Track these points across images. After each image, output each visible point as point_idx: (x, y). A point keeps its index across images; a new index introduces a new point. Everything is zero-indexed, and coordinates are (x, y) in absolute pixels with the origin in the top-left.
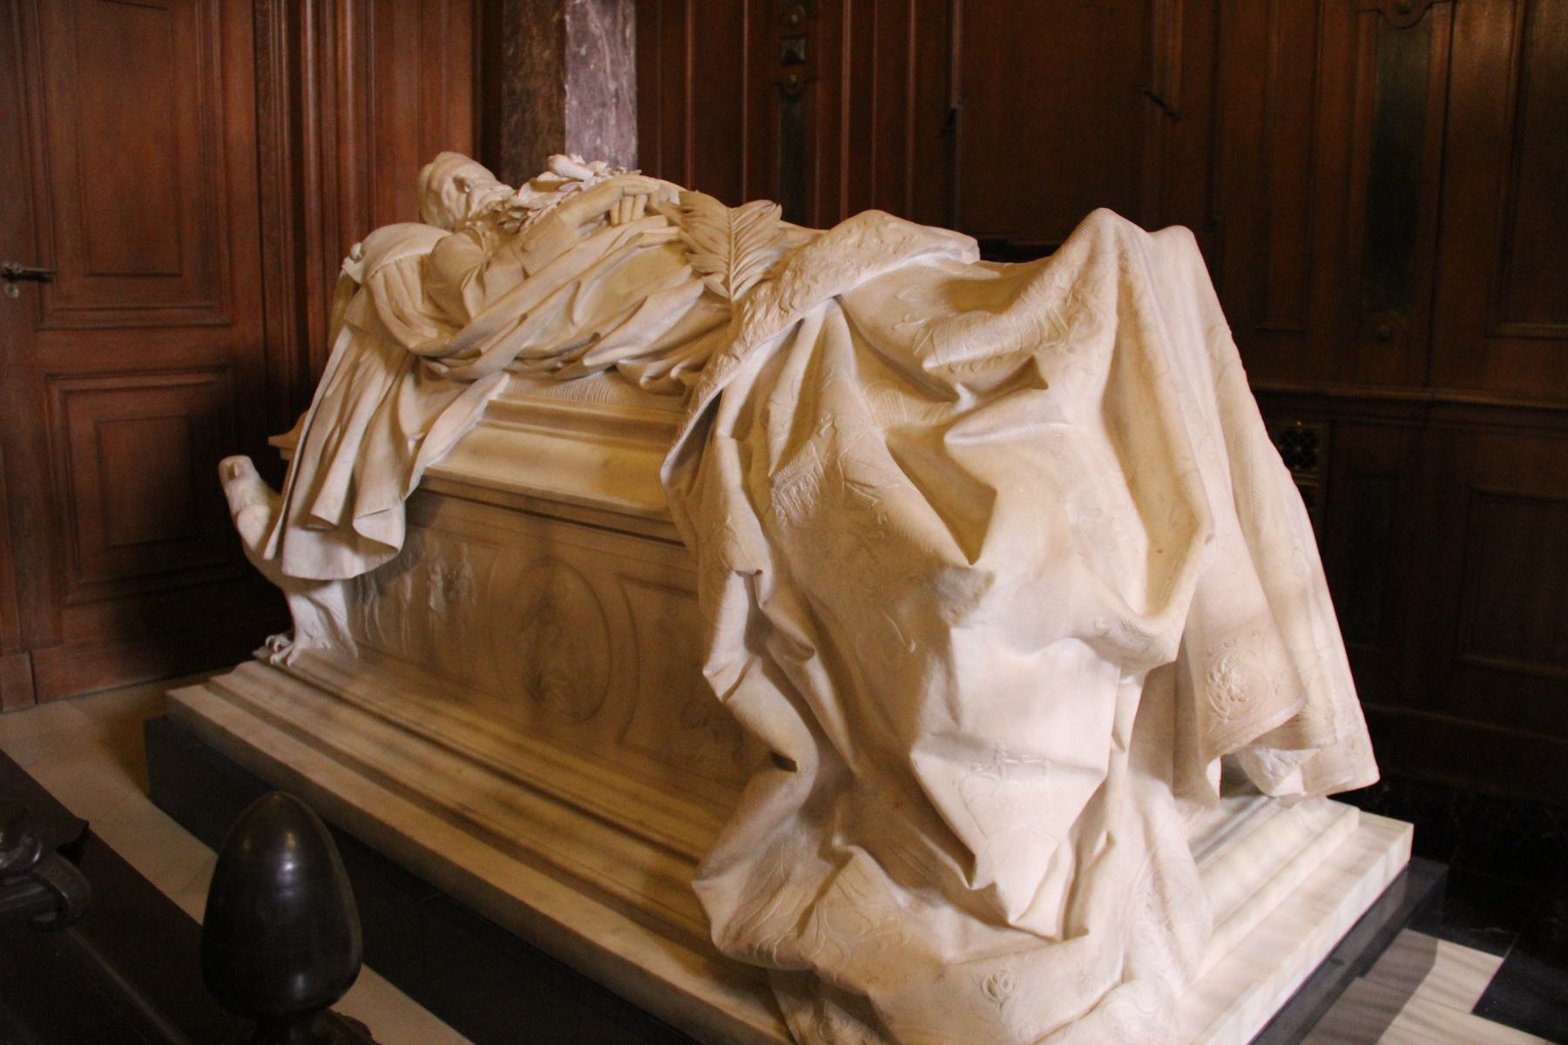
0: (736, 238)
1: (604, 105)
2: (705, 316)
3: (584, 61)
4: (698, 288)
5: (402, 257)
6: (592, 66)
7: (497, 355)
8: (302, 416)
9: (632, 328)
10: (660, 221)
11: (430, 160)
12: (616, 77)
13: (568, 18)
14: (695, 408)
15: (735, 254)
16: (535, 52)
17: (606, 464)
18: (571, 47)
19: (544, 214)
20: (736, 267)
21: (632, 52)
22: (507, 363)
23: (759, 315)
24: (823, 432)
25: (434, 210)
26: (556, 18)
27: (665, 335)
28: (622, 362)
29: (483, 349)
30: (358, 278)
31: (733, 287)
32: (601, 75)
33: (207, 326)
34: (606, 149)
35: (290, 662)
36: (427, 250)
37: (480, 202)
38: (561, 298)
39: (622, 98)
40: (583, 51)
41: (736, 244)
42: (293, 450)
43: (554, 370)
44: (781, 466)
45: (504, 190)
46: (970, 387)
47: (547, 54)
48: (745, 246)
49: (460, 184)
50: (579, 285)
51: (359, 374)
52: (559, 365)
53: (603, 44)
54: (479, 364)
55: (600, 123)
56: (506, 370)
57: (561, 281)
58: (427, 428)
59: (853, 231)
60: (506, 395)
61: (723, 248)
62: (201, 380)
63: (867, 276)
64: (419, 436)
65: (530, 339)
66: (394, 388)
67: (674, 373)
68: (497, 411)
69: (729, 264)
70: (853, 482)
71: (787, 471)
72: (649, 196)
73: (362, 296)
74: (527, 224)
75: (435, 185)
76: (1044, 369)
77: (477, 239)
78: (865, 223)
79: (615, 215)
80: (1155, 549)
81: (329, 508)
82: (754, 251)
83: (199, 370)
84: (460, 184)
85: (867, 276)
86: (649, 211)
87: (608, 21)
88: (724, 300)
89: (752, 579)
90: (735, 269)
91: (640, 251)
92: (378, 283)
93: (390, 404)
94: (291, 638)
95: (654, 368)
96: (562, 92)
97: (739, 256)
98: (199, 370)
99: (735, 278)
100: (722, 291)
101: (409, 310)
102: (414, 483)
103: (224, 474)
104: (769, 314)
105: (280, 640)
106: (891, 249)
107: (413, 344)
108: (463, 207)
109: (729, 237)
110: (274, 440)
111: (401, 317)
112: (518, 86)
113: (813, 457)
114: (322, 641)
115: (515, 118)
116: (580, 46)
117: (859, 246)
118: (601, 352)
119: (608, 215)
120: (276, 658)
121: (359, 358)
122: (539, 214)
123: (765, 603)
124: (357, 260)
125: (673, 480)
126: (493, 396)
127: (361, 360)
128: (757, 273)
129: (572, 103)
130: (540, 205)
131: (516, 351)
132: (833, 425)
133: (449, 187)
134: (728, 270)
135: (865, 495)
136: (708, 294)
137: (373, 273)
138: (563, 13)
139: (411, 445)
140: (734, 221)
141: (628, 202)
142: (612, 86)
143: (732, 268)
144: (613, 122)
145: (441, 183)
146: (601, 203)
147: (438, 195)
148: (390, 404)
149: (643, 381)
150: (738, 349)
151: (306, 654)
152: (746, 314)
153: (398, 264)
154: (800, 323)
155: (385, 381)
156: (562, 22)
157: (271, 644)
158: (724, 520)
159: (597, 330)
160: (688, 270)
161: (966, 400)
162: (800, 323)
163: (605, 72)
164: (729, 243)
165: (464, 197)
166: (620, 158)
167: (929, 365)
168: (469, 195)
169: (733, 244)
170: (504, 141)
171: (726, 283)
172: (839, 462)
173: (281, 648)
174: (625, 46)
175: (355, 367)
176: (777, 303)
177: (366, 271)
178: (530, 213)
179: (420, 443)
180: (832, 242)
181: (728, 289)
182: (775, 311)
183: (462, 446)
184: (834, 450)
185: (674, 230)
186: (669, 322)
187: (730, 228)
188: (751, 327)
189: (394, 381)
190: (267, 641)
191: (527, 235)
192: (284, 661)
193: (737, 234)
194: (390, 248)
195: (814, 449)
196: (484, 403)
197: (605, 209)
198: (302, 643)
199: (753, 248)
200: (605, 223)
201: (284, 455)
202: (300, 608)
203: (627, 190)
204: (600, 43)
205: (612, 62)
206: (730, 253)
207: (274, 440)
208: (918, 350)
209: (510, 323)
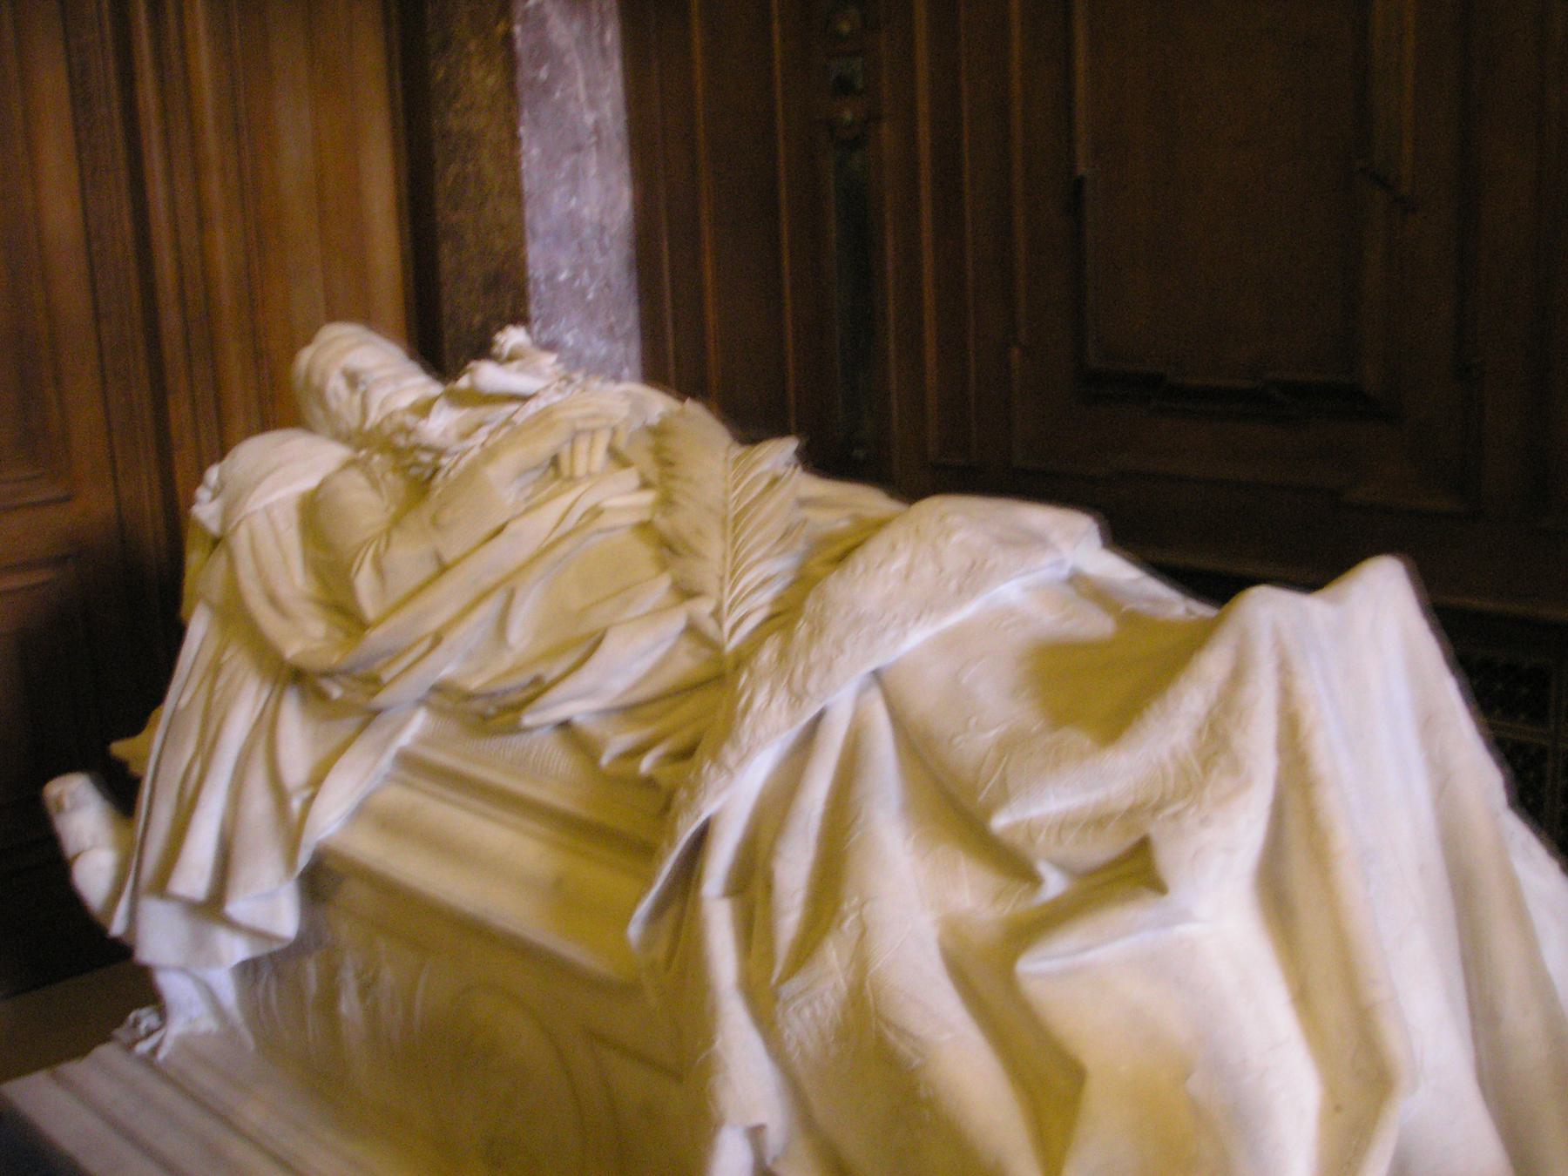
0: (735, 527)
1: (578, 148)
2: (687, 664)
3: (547, 88)
4: (677, 622)
5: (274, 498)
6: (558, 95)
7: (403, 690)
8: (153, 715)
9: (587, 677)
10: (630, 478)
11: (308, 341)
12: (593, 103)
13: (517, 29)
14: (672, 844)
15: (732, 564)
16: (477, 75)
17: (559, 882)
18: (525, 73)
19: (463, 463)
20: (733, 588)
21: (617, 64)
22: (421, 693)
23: (760, 700)
24: (847, 924)
25: (318, 413)
26: (501, 28)
27: (634, 687)
28: (578, 719)
29: (386, 676)
30: (214, 527)
31: (727, 626)
32: (572, 107)
33: (34, 505)
34: (586, 212)
35: (162, 1055)
36: (309, 483)
37: (382, 405)
38: (489, 609)
39: (605, 134)
40: (543, 74)
41: (734, 543)
42: (145, 758)
43: (485, 718)
44: (785, 978)
45: (416, 384)
46: (1061, 866)
47: (490, 81)
48: (748, 547)
49: (353, 379)
50: (511, 595)
51: (221, 683)
52: (491, 710)
53: (573, 59)
54: (382, 699)
55: (575, 176)
56: (421, 702)
57: (489, 580)
58: (317, 781)
59: (900, 546)
60: (423, 740)
61: (714, 548)
62: (33, 581)
63: (917, 637)
64: (306, 793)
65: (447, 666)
66: (272, 702)
67: (646, 764)
68: (410, 764)
69: (722, 579)
70: (888, 1024)
71: (795, 984)
72: (614, 431)
73: (220, 561)
74: (440, 477)
75: (316, 379)
76: (1168, 858)
77: (375, 485)
78: (917, 531)
79: (565, 463)
80: (1333, 1106)
81: (194, 877)
82: (759, 561)
83: (28, 566)
84: (353, 379)
85: (917, 637)
86: (617, 457)
87: (577, 26)
88: (715, 646)
89: (756, 1134)
90: (731, 593)
91: (600, 537)
92: (241, 542)
93: (266, 728)
94: (163, 1014)
95: (619, 741)
96: (515, 140)
97: (738, 566)
98: (28, 566)
99: (731, 606)
100: (710, 627)
101: (283, 592)
102: (303, 860)
103: (51, 805)
104: (774, 700)
105: (147, 1018)
106: (953, 585)
107: (293, 650)
108: (357, 413)
109: (724, 522)
110: (120, 748)
111: (273, 601)
112: (454, 123)
113: (834, 956)
114: (207, 1023)
115: (453, 169)
116: (538, 66)
117: (907, 576)
118: (544, 708)
119: (555, 461)
120: (143, 1047)
121: (222, 654)
122: (456, 463)
123: (775, 1160)
124: (216, 494)
125: (648, 942)
126: (405, 739)
127: (226, 657)
128: (762, 602)
129: (531, 153)
130: (456, 447)
131: (433, 680)
132: (860, 917)
133: (336, 384)
134: (721, 590)
135: (904, 1048)
136: (692, 629)
137: (234, 524)
138: (512, 25)
139: (296, 804)
140: (734, 491)
141: (582, 446)
142: (589, 119)
143: (727, 590)
144: (593, 171)
145: (325, 377)
146: (544, 447)
147: (320, 394)
148: (266, 728)
149: (605, 760)
150: (731, 757)
151: (184, 1044)
152: (741, 695)
153: (268, 510)
154: (819, 717)
155: (258, 694)
156: (508, 39)
157: (137, 1023)
158: (713, 1042)
159: (540, 669)
160: (663, 583)
161: (1054, 884)
162: (819, 717)
163: (577, 99)
164: (724, 537)
165: (357, 399)
166: (607, 221)
167: (1000, 822)
168: (365, 397)
169: (730, 540)
170: (440, 204)
171: (716, 614)
172: (867, 984)
173: (150, 1033)
174: (603, 51)
175: (215, 669)
176: (785, 680)
177: (226, 514)
178: (445, 461)
179: (309, 802)
180: (866, 570)
181: (720, 625)
182: (782, 698)
183: (362, 812)
184: (860, 962)
185: (648, 497)
186: (642, 666)
187: (725, 505)
188: (748, 720)
189: (271, 693)
190: (132, 1016)
191: (440, 496)
192: (155, 1050)
193: (737, 518)
194: (258, 483)
195: (834, 953)
196: (392, 751)
197: (553, 454)
198: (177, 1027)
199: (757, 555)
200: (551, 472)
201: (134, 769)
202: (173, 985)
203: (579, 425)
204: (567, 60)
205: (587, 85)
206: (724, 557)
207: (120, 748)
208: (985, 792)
209: (421, 640)
